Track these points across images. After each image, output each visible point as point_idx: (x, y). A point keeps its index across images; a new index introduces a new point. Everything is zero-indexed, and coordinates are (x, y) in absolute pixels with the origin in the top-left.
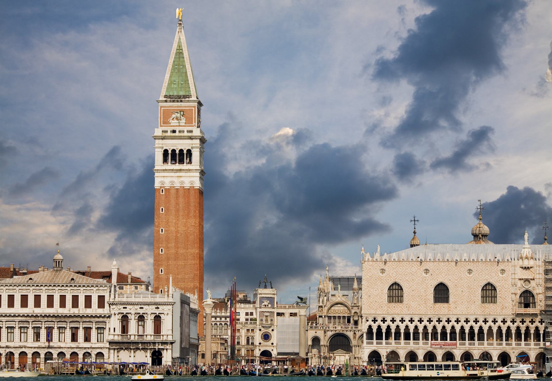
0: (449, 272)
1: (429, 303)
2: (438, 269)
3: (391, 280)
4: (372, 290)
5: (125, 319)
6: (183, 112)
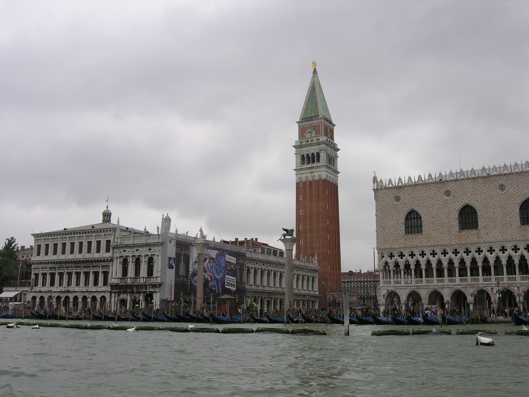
0: (475, 191)
1: (454, 231)
2: (461, 189)
4: (386, 221)
5: (125, 262)
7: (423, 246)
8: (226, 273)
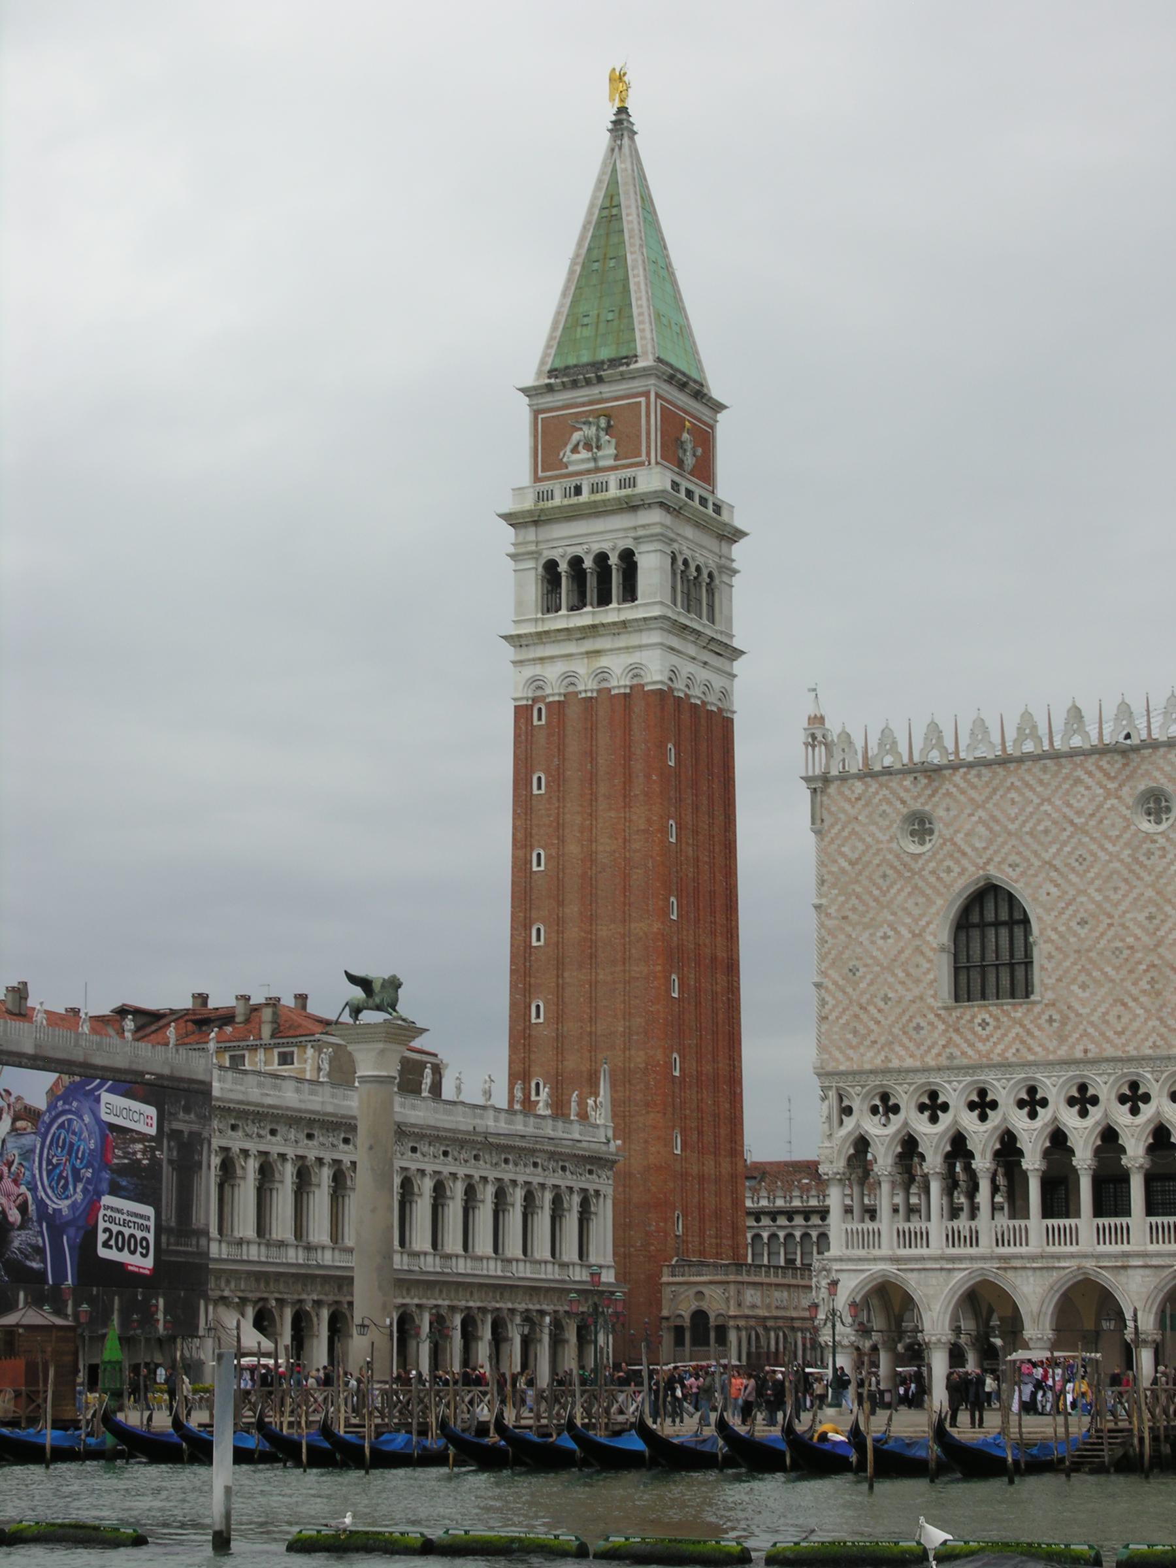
3: (963, 871)
4: (865, 937)
6: (608, 417)
7: (1035, 1064)
8: (105, 1186)
